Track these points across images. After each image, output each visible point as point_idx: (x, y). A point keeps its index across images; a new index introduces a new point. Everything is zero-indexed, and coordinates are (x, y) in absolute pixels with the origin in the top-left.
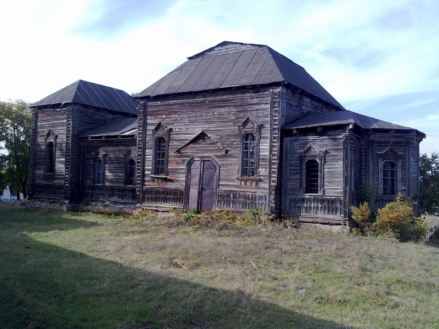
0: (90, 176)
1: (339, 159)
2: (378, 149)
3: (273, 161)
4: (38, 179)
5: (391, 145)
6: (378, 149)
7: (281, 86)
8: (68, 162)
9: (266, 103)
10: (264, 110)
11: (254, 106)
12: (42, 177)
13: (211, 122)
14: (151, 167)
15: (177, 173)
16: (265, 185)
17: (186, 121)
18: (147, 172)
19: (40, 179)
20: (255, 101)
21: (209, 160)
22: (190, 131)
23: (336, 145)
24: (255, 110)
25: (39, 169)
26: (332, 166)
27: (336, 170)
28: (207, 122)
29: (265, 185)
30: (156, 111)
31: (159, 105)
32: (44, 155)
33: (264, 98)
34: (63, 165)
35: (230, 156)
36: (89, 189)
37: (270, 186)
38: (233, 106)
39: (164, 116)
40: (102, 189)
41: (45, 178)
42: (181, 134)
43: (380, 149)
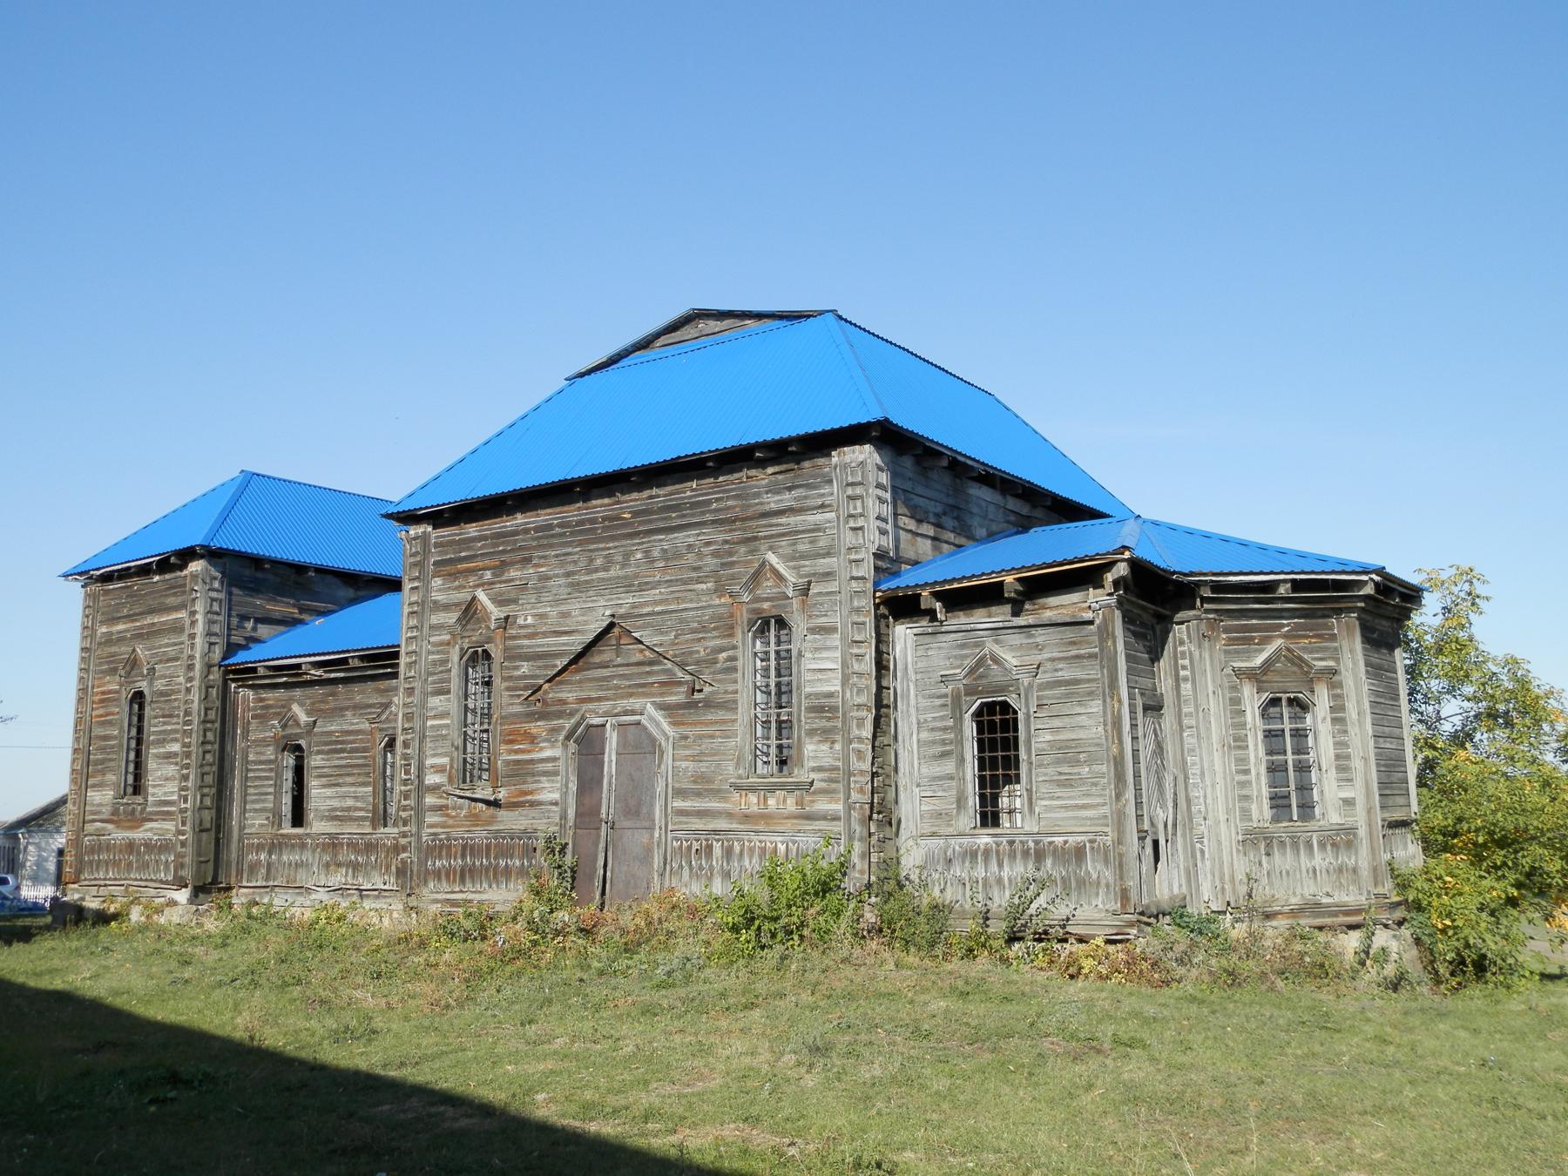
0: (264, 801)
1: (1090, 693)
2: (1237, 652)
3: (855, 714)
4: (94, 821)
5: (1285, 636)
6: (1237, 652)
7: (869, 441)
8: (188, 755)
9: (823, 506)
10: (818, 530)
11: (783, 520)
12: (106, 812)
13: (642, 587)
14: (445, 760)
15: (533, 775)
16: (833, 806)
17: (559, 584)
18: (431, 779)
19: (102, 821)
20: (787, 499)
21: (638, 723)
22: (569, 624)
23: (1074, 643)
24: (783, 535)
25: (101, 785)
26: (1067, 720)
27: (1082, 734)
28: (628, 585)
29: (833, 806)
30: (465, 559)
31: (474, 539)
32: (115, 738)
33: (816, 487)
34: (173, 767)
35: (709, 704)
36: (260, 848)
37: (849, 808)
38: (713, 522)
39: (488, 575)
40: (303, 846)
41: (116, 818)
42: (545, 634)
43: (1244, 652)
